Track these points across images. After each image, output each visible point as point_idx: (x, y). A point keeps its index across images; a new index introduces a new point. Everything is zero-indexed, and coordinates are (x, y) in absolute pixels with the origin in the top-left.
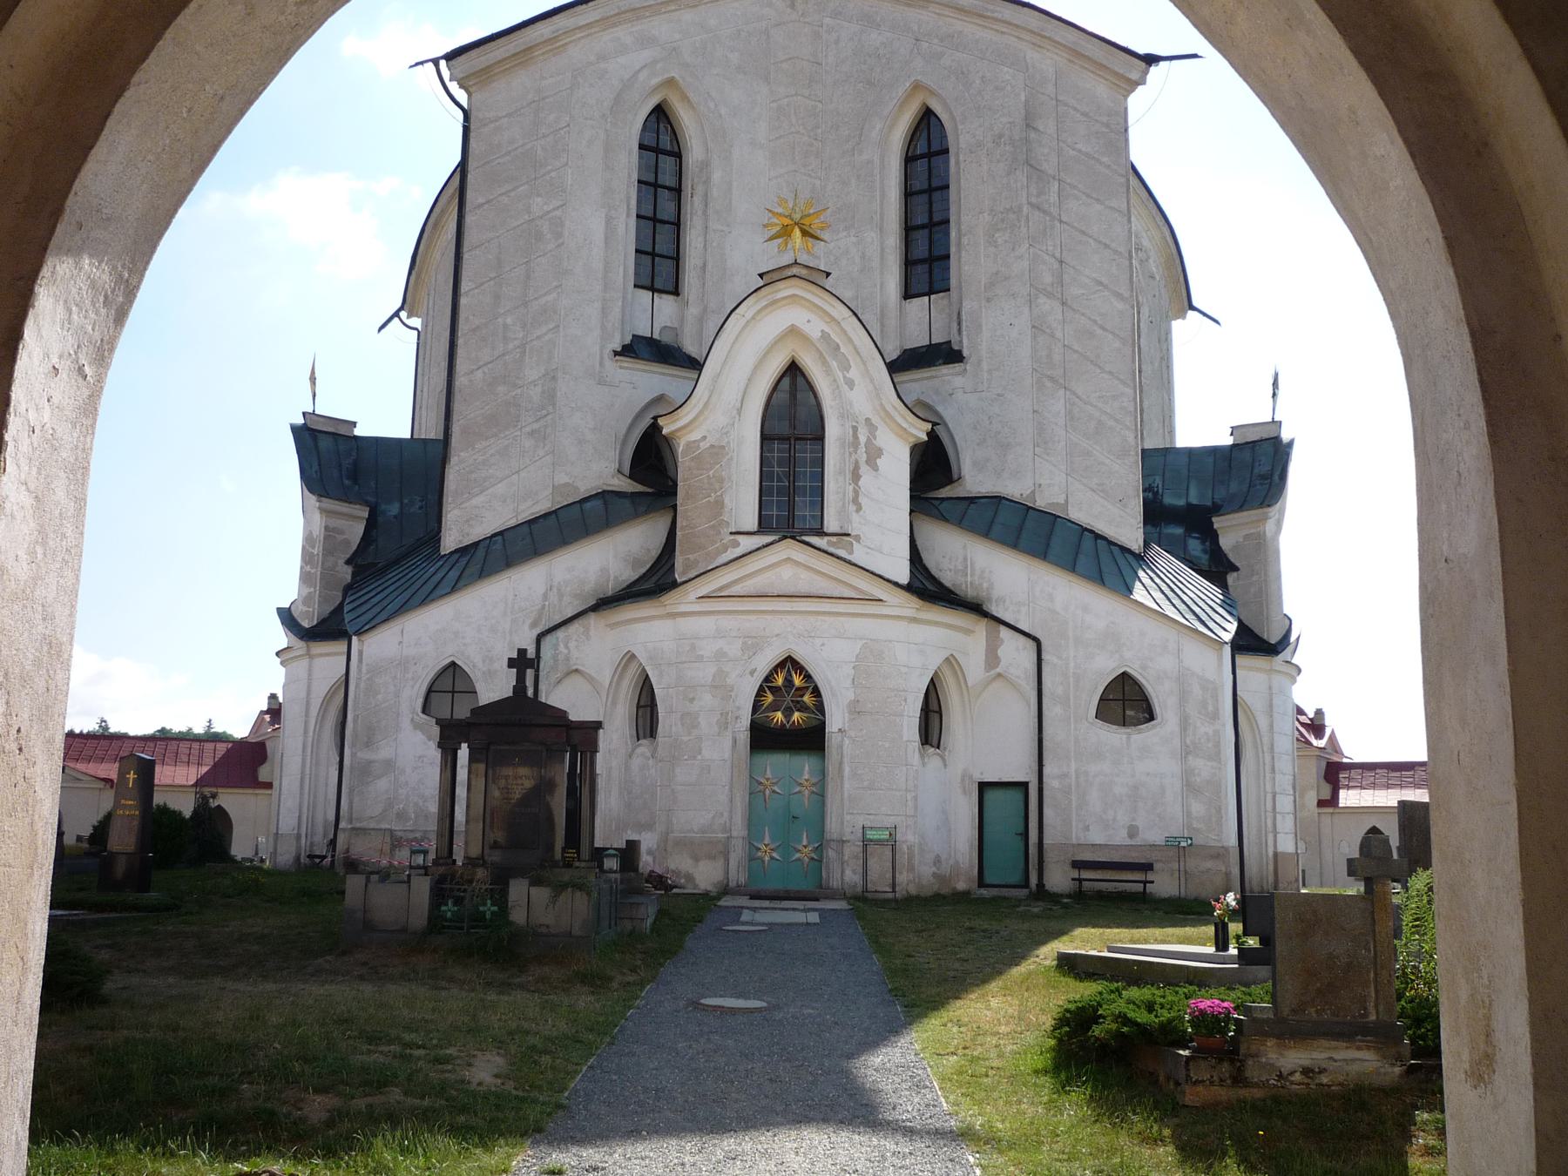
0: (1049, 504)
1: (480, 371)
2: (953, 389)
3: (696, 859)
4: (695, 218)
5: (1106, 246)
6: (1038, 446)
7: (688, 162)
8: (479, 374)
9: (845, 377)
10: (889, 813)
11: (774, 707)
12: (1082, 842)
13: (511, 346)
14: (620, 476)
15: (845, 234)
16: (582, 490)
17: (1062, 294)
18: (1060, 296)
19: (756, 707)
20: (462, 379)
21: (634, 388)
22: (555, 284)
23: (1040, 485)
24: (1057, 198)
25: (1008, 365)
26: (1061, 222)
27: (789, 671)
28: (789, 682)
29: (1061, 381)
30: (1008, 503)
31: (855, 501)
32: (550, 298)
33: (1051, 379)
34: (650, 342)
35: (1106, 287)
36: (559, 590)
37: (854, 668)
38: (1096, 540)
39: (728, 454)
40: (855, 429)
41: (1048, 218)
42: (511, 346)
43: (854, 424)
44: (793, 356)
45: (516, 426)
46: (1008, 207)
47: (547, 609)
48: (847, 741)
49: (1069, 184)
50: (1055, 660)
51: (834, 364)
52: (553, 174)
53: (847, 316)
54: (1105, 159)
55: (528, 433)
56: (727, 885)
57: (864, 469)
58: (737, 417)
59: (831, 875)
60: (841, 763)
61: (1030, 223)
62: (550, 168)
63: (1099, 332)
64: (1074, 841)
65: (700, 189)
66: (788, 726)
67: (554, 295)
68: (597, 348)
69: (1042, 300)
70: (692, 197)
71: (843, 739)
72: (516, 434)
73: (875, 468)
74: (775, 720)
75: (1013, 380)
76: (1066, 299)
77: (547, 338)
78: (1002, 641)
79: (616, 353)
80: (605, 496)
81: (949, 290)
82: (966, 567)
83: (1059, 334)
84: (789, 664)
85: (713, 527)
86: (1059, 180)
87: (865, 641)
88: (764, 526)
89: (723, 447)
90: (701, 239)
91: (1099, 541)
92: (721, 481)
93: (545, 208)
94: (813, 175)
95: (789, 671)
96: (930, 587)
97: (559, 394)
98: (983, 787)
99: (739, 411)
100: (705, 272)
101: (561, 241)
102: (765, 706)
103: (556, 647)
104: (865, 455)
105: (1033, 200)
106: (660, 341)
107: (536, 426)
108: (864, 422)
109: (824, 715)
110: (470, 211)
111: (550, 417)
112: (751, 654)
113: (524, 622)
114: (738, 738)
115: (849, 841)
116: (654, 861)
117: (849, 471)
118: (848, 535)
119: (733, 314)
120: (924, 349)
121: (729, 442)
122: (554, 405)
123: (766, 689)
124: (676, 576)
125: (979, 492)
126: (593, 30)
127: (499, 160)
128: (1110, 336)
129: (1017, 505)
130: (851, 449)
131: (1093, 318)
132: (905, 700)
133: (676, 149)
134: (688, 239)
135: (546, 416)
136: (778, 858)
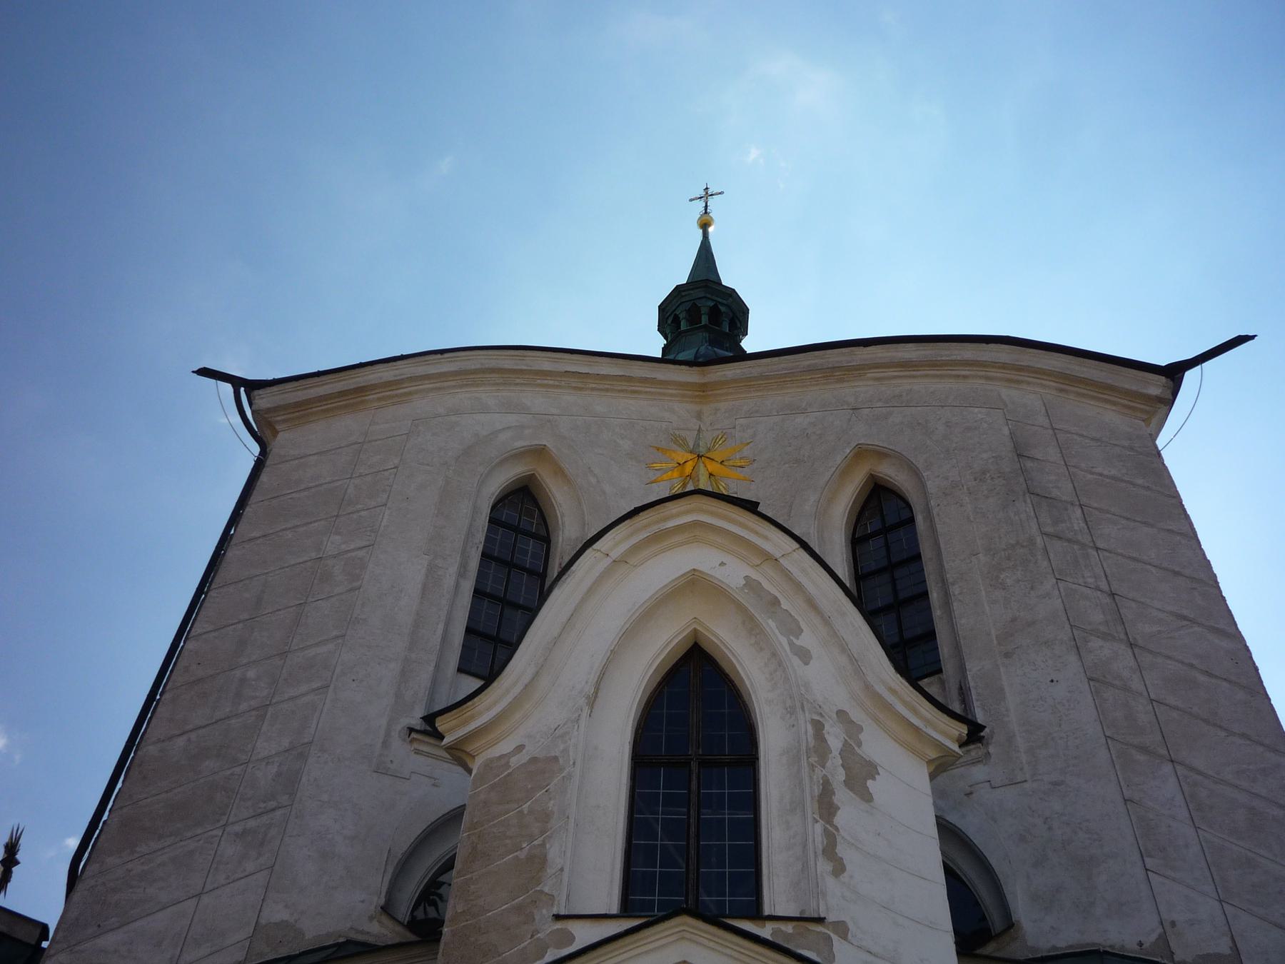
1: (185, 737)
2: (971, 786)
5: (1177, 574)
7: (558, 542)
8: (181, 742)
9: (791, 644)
13: (244, 706)
14: (385, 919)
17: (1126, 634)
18: (1122, 636)
20: (151, 748)
21: (434, 785)
22: (335, 633)
25: (1061, 738)
26: (1097, 549)
31: (830, 851)
33: (1143, 749)
35: (1192, 621)
39: (562, 770)
40: (818, 727)
41: (1075, 547)
42: (244, 706)
43: (816, 717)
44: (695, 630)
45: (218, 821)
46: (1012, 542)
49: (1096, 508)
51: (771, 625)
52: (363, 513)
53: (790, 550)
55: (237, 834)
57: (842, 796)
58: (586, 710)
61: (1052, 556)
62: (360, 506)
67: (331, 646)
69: (1095, 643)
72: (214, 832)
73: (867, 797)
76: (1135, 639)
81: (940, 671)
83: (1136, 684)
85: (519, 909)
86: (1081, 505)
88: (627, 908)
89: (556, 759)
92: (546, 817)
93: (343, 547)
97: (304, 779)
99: (592, 701)
101: (356, 584)
104: (841, 771)
105: (1049, 529)
107: (252, 823)
108: (835, 716)
110: (236, 545)
111: (279, 813)
117: (812, 798)
118: (820, 920)
119: (589, 552)
121: (566, 751)
125: (1054, 948)
126: (446, 384)
128: (1225, 684)
130: (813, 759)
133: (543, 533)
135: (273, 810)
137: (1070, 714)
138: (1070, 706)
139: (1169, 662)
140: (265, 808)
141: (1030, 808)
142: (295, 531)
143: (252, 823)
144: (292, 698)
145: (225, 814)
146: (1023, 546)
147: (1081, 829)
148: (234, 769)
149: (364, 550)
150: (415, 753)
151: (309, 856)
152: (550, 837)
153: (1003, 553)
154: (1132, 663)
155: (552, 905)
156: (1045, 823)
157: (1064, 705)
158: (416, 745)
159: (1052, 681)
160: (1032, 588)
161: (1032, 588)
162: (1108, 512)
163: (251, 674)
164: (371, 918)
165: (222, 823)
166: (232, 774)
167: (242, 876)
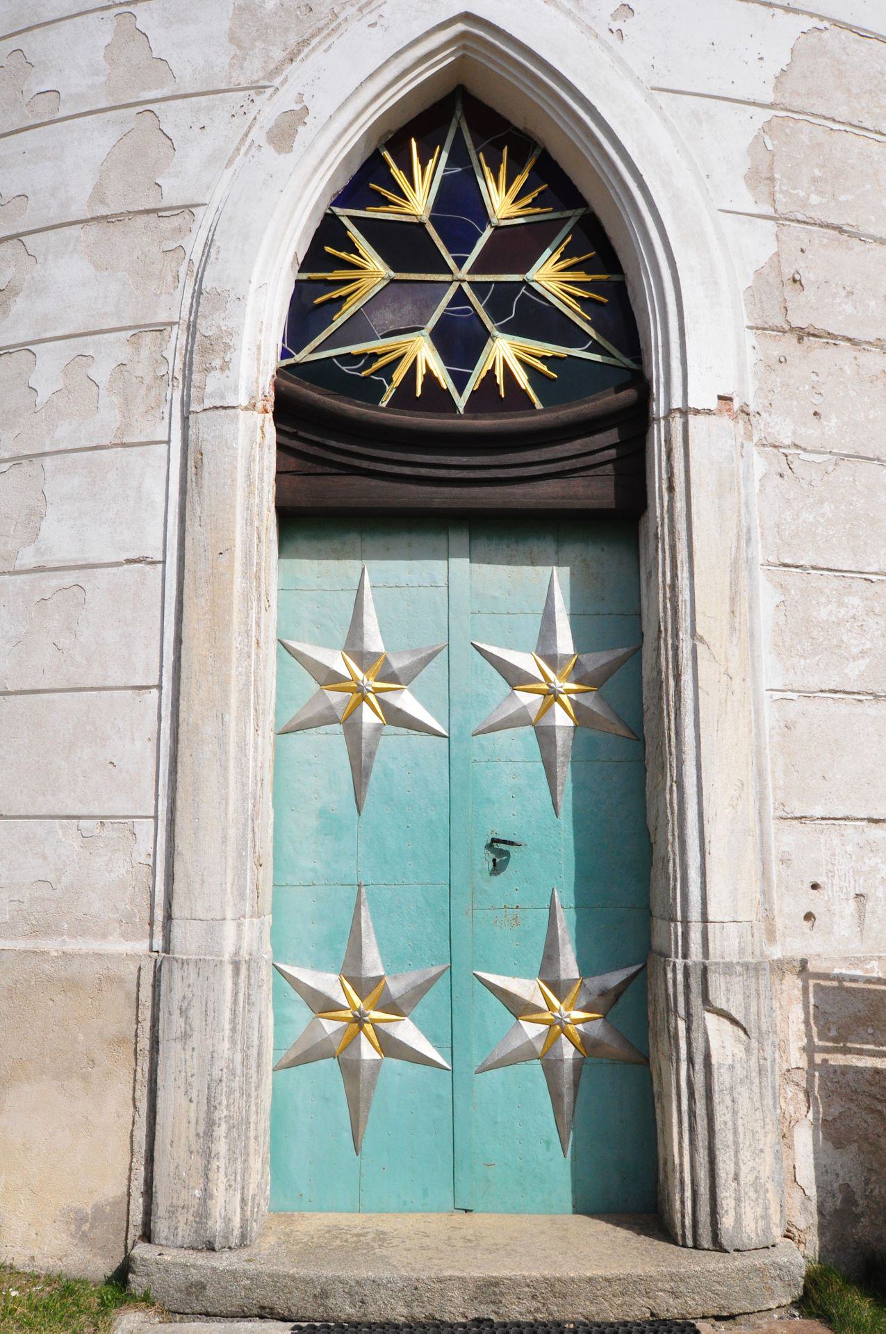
60: (738, 565)
66: (461, 402)
74: (399, 375)
84: (458, 123)
87: (815, 22)
102: (349, 309)
112: (278, 54)
123: (354, 233)
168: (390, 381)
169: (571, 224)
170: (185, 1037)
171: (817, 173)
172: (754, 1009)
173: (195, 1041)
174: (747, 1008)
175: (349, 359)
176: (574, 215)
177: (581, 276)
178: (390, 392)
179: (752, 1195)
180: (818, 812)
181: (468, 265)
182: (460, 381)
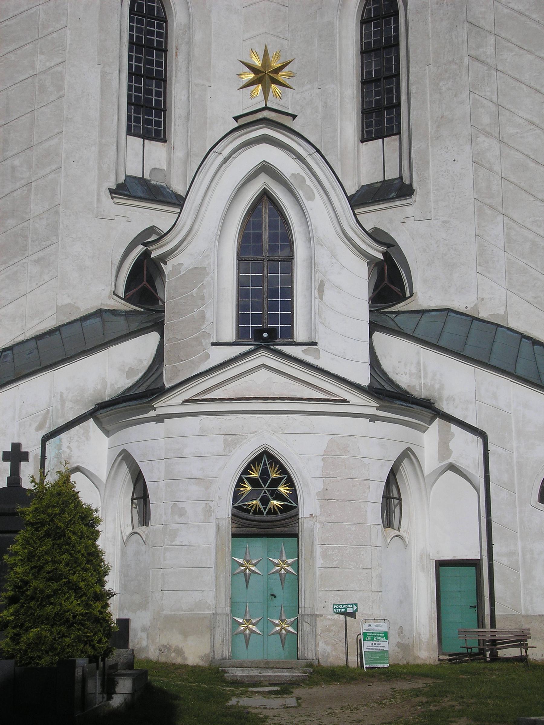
0: (490, 315)
3: (185, 634)
4: (179, 74)
5: (537, 91)
6: (480, 265)
7: (173, 26)
10: (357, 589)
11: (252, 496)
12: (530, 613)
14: (115, 297)
15: (309, 86)
16: (82, 310)
18: (497, 135)
19: (236, 496)
22: (57, 130)
23: (483, 299)
24: (493, 50)
27: (265, 464)
28: (265, 474)
29: (500, 209)
30: (454, 315)
32: (52, 142)
34: (142, 182)
36: (61, 396)
37: (322, 459)
38: (533, 346)
41: (486, 68)
42: (18, 185)
45: (24, 254)
47: (50, 414)
48: (318, 526)
50: (500, 451)
54: (534, 16)
55: (35, 261)
56: (214, 658)
59: (306, 648)
60: (312, 546)
61: (470, 72)
63: (532, 165)
64: (523, 613)
65: (183, 49)
66: (265, 514)
67: (56, 140)
68: (95, 186)
69: (482, 138)
70: (176, 56)
71: (314, 524)
72: (24, 261)
74: (253, 508)
75: (457, 209)
76: (503, 137)
77: (50, 177)
78: (453, 435)
79: (111, 191)
80: (100, 313)
82: (420, 371)
83: (497, 168)
84: (265, 457)
90: (184, 92)
91: (536, 347)
94: (281, 36)
95: (265, 464)
96: (388, 388)
97: (61, 226)
98: (441, 564)
100: (188, 121)
101: (61, 93)
102: (244, 496)
103: (59, 447)
105: (472, 53)
106: (149, 181)
109: (297, 502)
113: (30, 425)
114: (220, 525)
115: (321, 616)
116: (148, 638)
120: (379, 185)
121: (209, 264)
122: (57, 236)
123: (245, 480)
124: (165, 382)
127: (7, 23)
129: (463, 317)
131: (526, 153)
132: (369, 487)
134: (173, 92)
136: (258, 632)
137: (459, 183)
138: (460, 177)
139: (516, 153)
140: (45, 245)
141: (431, 235)
142: (15, 54)
143: (41, 254)
144: (43, 177)
145: (26, 250)
146: (456, 63)
147: (452, 248)
148: (24, 224)
149: (61, 65)
150: (115, 204)
151: (74, 269)
152: (206, 307)
153: (444, 66)
154: (498, 153)
155: (210, 338)
156: (436, 243)
157: (457, 177)
158: (115, 200)
159: (455, 160)
160: (455, 96)
161: (455, 96)
162: (509, 41)
163: (17, 162)
164: (109, 298)
165: (26, 255)
166: (24, 227)
167: (43, 282)
168: (252, 509)
169: (286, 478)
170: (219, 626)
171: (332, 467)
172: (312, 622)
173: (220, 627)
174: (311, 622)
175: (244, 505)
176: (286, 476)
177: (288, 488)
178: (252, 511)
179: (310, 651)
180: (326, 589)
181: (266, 486)
182: (265, 509)
